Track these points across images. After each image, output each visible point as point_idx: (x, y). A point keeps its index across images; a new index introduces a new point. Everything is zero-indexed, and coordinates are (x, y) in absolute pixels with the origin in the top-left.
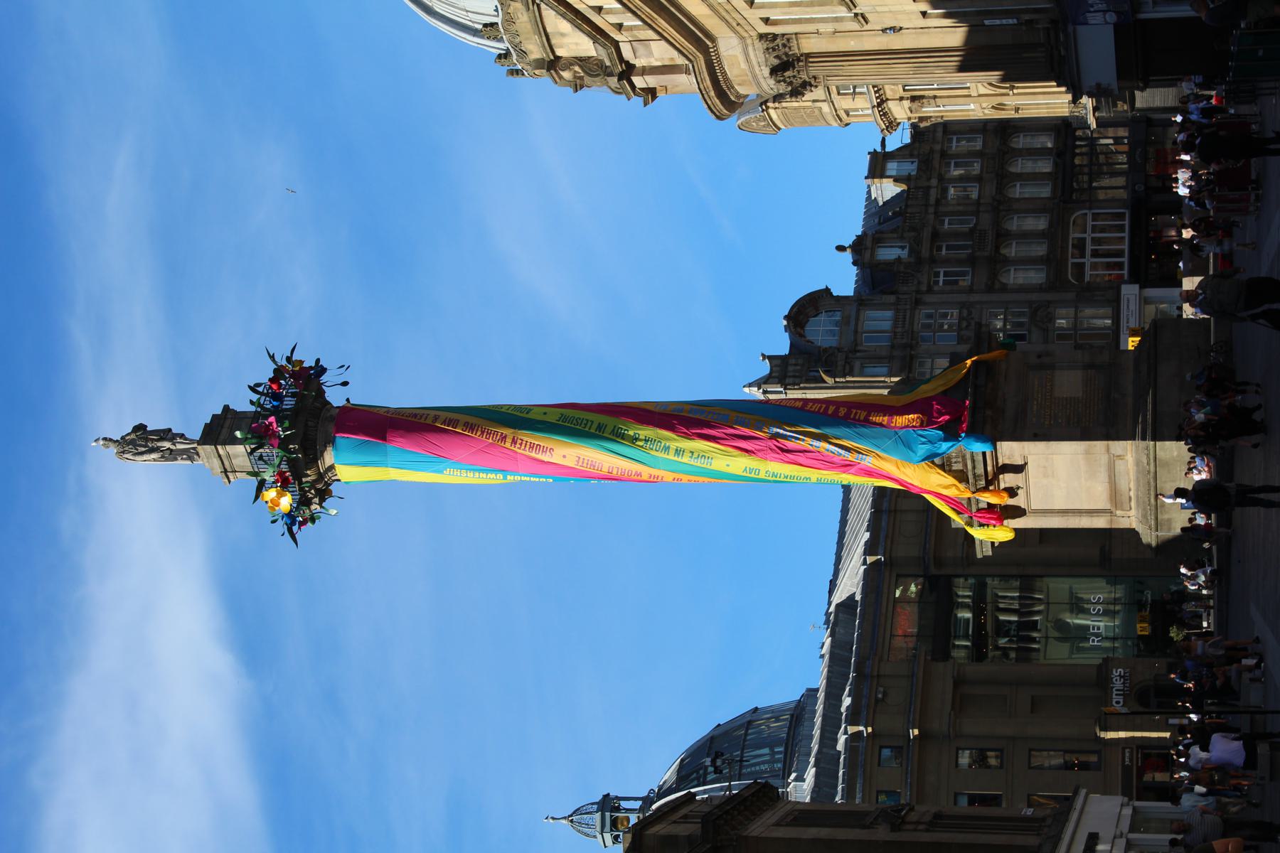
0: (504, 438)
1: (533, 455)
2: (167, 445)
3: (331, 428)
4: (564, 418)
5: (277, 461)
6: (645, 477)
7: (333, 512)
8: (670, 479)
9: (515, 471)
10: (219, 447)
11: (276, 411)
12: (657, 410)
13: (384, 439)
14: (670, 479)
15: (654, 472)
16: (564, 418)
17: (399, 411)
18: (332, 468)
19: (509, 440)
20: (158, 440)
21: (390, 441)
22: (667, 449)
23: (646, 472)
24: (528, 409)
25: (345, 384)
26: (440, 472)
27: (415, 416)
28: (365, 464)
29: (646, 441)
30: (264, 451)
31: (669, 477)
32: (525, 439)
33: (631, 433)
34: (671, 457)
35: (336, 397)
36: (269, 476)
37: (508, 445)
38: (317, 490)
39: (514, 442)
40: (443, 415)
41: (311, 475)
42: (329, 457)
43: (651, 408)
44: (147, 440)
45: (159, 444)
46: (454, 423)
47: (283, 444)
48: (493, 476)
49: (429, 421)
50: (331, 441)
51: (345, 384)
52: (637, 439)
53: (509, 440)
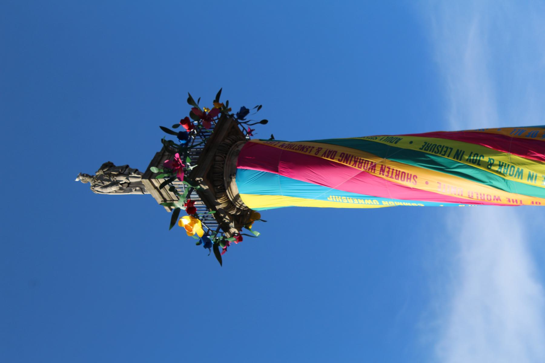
0: (373, 167)
1: (399, 182)
2: (123, 179)
3: (235, 161)
4: (427, 146)
5: (186, 193)
6: (506, 202)
7: (257, 234)
8: (529, 203)
9: (387, 197)
10: (153, 180)
11: (183, 150)
12: (512, 135)
13: (276, 170)
14: (529, 203)
15: (512, 196)
16: (427, 146)
17: (291, 145)
18: (238, 196)
19: (378, 169)
20: (117, 175)
21: (281, 173)
22: (520, 174)
23: (504, 196)
24: (397, 139)
25: (264, 122)
26: (324, 198)
27: (302, 148)
28: (262, 193)
29: (500, 166)
30: (176, 183)
31: (527, 200)
32: (392, 167)
33: (486, 159)
34: (525, 181)
35: (260, 134)
36: (180, 205)
37: (377, 173)
38: (230, 215)
39: (382, 170)
40: (325, 147)
41: (221, 204)
42: (235, 188)
43: (505, 133)
44: (110, 175)
45: (118, 178)
46: (332, 154)
47: (190, 178)
48: (369, 201)
49: (313, 154)
50: (233, 174)
51: (264, 122)
52: (491, 165)
53: (378, 169)
